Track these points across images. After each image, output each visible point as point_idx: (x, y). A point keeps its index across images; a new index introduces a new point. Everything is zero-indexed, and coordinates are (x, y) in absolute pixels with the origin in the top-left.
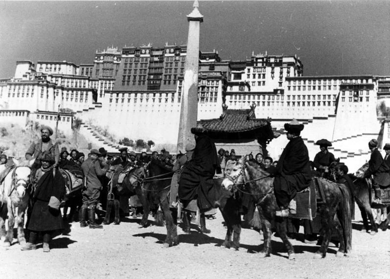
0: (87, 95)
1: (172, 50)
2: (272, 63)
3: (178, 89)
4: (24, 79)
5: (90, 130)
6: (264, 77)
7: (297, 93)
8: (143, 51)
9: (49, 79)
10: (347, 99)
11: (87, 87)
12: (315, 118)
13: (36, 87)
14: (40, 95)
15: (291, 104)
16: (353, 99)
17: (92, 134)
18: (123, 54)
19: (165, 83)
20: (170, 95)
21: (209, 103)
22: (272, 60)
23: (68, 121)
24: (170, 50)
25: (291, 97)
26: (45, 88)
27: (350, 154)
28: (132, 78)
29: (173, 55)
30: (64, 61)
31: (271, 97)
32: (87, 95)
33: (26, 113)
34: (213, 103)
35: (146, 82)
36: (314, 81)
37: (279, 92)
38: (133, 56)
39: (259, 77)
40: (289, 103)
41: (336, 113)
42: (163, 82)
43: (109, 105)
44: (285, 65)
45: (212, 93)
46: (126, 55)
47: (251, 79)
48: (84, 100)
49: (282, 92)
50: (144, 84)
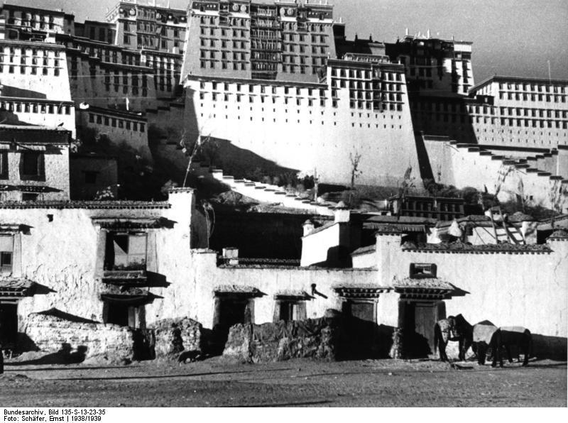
1: (290, 11)
3: (329, 82)
7: (513, 103)
8: (235, 7)
11: (120, 63)
12: (560, 147)
15: (507, 122)
18: (194, 7)
19: (284, 69)
20: (316, 93)
21: (388, 112)
23: (142, 130)
24: (286, 11)
25: (506, 111)
28: (218, 56)
29: (294, 19)
30: (59, 10)
34: (396, 113)
35: (249, 66)
36: (554, 86)
37: (486, 100)
40: (503, 120)
42: (280, 67)
44: (459, 56)
45: (391, 98)
46: (202, 10)
48: (141, 91)
49: (491, 99)
50: (243, 68)
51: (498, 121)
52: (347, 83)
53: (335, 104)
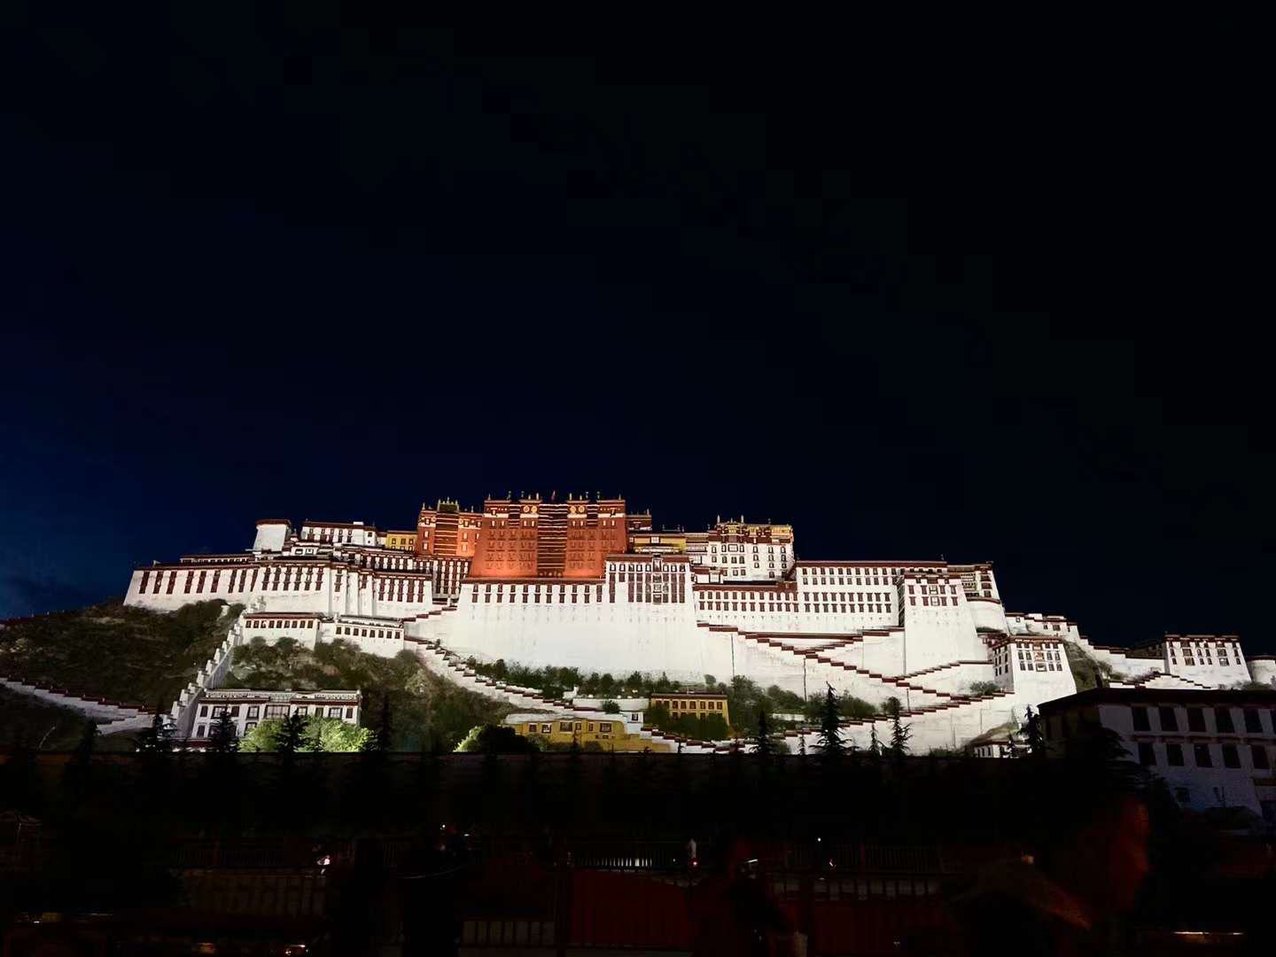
0: (421, 585)
1: (582, 509)
2: (753, 538)
4: (286, 554)
5: (443, 656)
6: (742, 561)
7: (820, 588)
8: (526, 508)
9: (337, 554)
10: (919, 601)
11: (410, 567)
13: (326, 570)
14: (334, 587)
16: (929, 600)
17: (447, 662)
20: (593, 588)
22: (753, 535)
24: (577, 508)
25: (811, 597)
26: (344, 572)
27: (953, 698)
31: (775, 595)
32: (421, 585)
33: (316, 622)
38: (506, 516)
39: (734, 561)
41: (901, 625)
43: (470, 609)
47: (719, 564)
48: (416, 598)
49: (793, 588)
51: (802, 608)
52: (627, 577)
53: (612, 600)
